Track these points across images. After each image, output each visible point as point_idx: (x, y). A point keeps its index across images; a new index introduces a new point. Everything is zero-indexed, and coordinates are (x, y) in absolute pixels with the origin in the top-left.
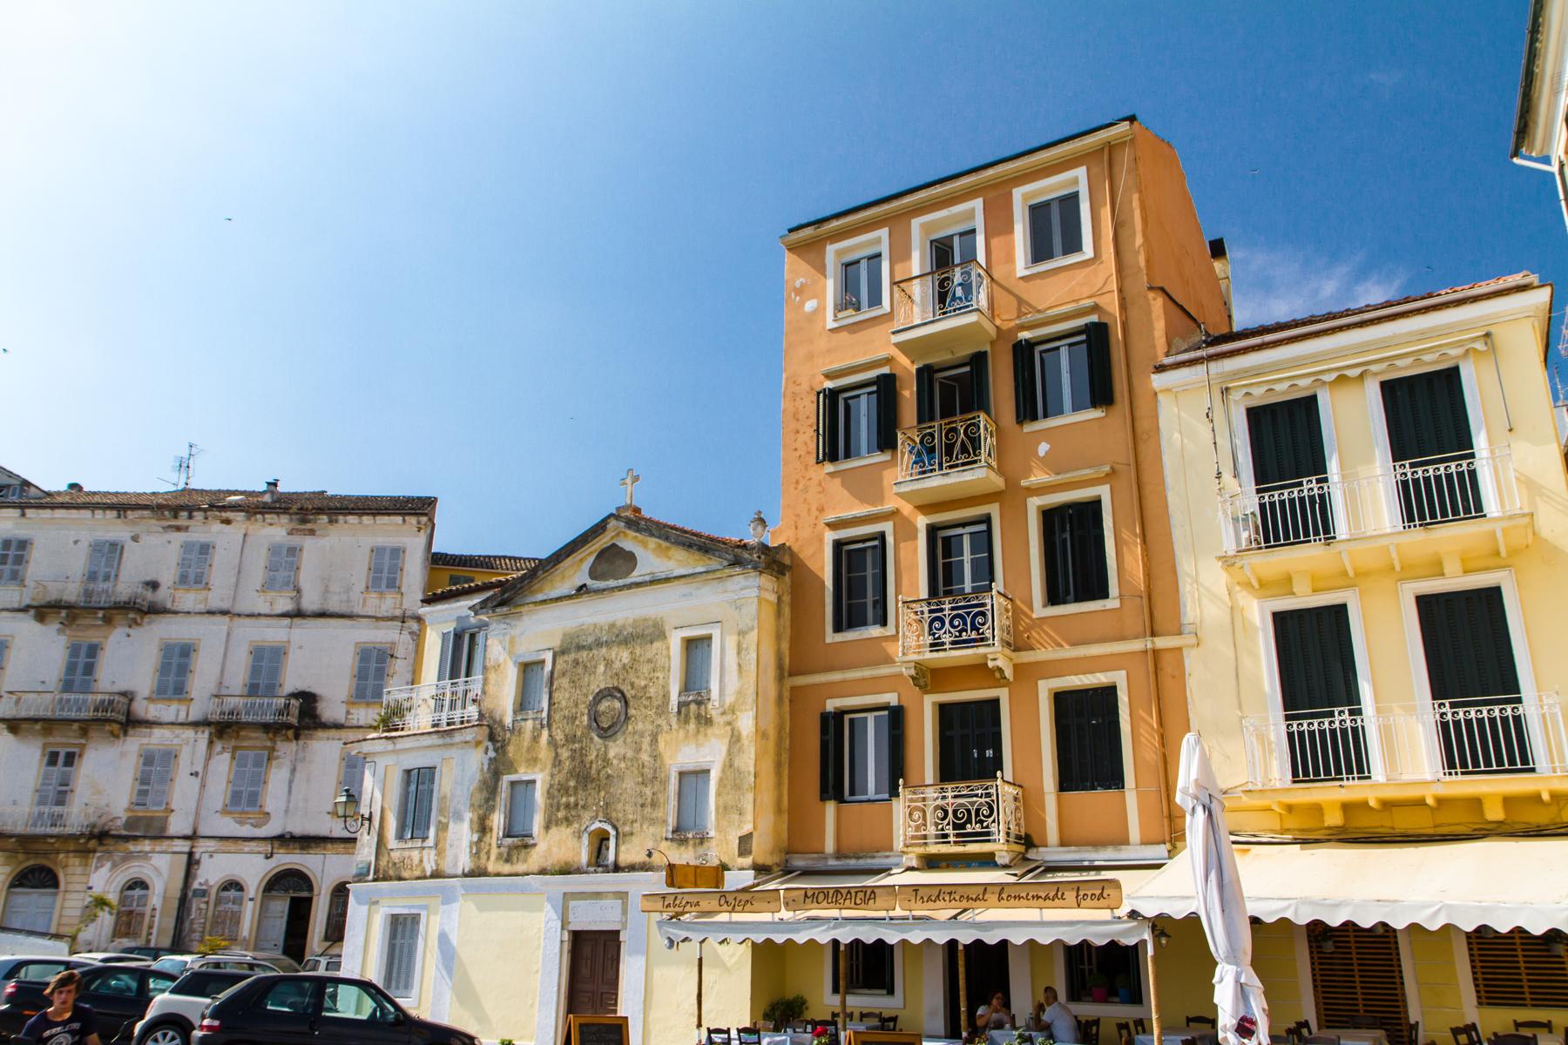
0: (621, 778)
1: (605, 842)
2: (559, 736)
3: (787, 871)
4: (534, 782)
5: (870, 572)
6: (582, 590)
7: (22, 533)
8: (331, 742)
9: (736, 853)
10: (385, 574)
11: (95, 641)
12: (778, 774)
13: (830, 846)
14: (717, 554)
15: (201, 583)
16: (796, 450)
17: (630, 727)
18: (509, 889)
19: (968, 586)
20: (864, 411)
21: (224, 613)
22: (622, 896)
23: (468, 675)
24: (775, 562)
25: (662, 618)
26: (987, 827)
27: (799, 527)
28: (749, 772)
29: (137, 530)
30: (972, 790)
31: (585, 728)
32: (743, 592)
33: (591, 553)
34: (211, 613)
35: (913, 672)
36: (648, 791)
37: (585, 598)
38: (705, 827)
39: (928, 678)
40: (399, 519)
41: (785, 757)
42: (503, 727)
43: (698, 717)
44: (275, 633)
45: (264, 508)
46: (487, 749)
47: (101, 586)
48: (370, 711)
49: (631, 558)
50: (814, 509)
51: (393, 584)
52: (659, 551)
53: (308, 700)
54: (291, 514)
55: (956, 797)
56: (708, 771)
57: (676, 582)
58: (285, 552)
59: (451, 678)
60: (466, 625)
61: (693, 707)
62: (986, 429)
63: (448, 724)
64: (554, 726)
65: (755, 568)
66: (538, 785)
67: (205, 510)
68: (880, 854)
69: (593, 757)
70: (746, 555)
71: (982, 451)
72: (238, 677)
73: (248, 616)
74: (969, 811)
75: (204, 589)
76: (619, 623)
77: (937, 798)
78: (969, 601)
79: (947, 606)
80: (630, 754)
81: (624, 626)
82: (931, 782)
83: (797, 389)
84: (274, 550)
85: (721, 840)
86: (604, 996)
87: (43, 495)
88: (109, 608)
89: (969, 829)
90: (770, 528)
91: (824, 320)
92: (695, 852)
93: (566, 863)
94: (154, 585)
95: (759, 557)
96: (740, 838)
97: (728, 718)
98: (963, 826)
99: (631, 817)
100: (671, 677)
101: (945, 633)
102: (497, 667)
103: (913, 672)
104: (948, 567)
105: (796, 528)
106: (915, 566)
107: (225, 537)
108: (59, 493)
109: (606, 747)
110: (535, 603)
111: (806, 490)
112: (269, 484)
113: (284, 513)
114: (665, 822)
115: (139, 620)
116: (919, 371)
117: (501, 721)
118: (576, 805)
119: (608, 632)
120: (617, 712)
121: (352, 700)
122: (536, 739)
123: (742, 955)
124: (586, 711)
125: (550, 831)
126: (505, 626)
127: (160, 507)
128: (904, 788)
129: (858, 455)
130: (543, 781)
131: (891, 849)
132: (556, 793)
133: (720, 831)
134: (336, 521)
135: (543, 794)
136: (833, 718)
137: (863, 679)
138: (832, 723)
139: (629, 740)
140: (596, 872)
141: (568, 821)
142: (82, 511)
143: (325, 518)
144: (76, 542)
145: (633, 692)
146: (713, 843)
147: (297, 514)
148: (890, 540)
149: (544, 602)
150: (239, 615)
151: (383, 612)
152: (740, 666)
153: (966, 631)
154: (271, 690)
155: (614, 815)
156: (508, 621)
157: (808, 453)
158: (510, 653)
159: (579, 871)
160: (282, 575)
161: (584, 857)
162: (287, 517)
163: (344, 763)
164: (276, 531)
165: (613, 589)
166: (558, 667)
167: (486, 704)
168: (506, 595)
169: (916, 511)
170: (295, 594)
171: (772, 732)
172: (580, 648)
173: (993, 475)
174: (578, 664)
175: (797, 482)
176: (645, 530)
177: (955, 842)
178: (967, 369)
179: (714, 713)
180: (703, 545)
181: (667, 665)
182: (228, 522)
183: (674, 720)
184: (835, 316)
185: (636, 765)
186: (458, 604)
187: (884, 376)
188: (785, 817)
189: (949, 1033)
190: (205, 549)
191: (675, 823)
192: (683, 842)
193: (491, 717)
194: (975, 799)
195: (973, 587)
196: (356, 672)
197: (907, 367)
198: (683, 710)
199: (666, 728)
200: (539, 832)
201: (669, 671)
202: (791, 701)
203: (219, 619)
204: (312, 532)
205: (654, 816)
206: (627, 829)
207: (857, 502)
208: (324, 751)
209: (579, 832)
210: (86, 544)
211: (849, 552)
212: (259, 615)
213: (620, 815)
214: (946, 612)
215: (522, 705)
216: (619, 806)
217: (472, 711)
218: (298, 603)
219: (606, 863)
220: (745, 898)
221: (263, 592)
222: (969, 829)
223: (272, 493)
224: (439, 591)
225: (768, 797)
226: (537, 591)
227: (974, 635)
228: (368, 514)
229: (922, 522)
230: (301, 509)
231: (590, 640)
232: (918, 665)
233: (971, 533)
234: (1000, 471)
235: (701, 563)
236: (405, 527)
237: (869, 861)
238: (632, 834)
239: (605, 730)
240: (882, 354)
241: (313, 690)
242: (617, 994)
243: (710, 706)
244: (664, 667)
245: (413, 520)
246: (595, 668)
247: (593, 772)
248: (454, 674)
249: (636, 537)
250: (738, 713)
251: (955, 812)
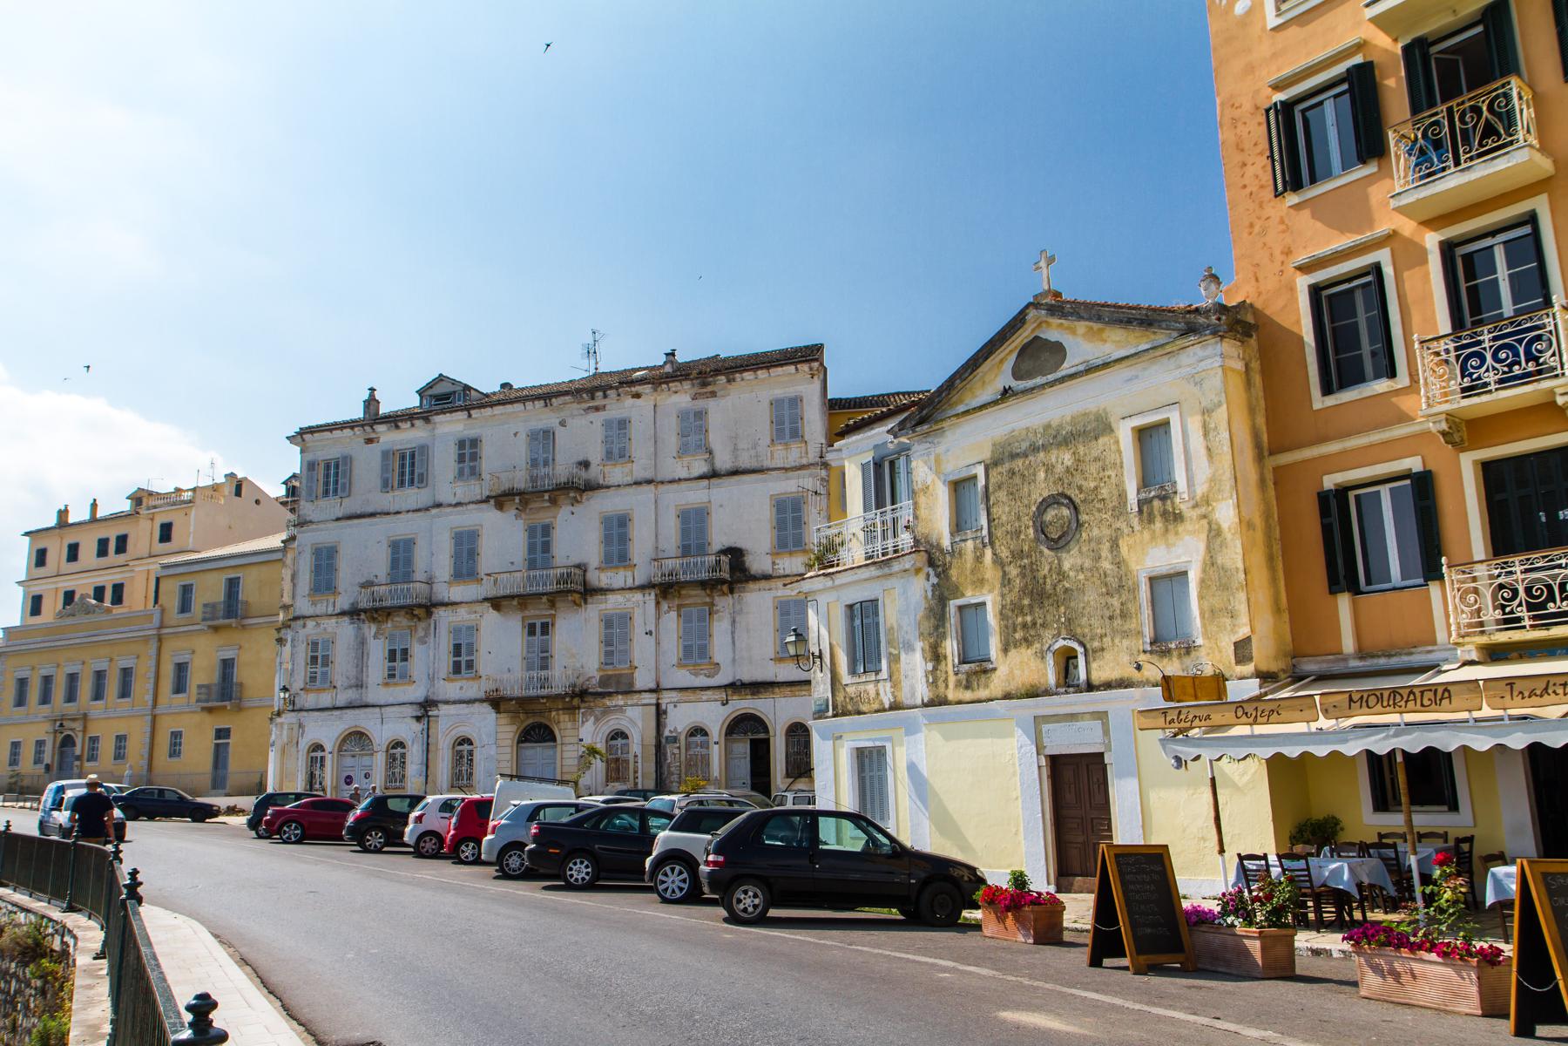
0: (1082, 591)
1: (1071, 661)
2: (1004, 553)
3: (1297, 678)
4: (984, 604)
5: (1362, 318)
6: (1006, 393)
7: (472, 433)
8: (763, 592)
9: (1233, 661)
10: (787, 426)
11: (547, 521)
12: (1272, 568)
13: (1348, 644)
14: (1164, 325)
15: (624, 456)
16: (1245, 186)
17: (1084, 535)
18: (972, 718)
19: (1508, 308)
20: (1332, 122)
21: (649, 482)
22: (1102, 716)
23: (893, 503)
24: (1238, 322)
25: (1104, 409)
26: (1512, 612)
27: (1261, 278)
28: (1237, 569)
29: (563, 414)
30: (1552, 560)
31: (1032, 541)
32: (1203, 363)
33: (1011, 351)
34: (637, 483)
35: (1444, 426)
36: (1115, 602)
37: (1012, 401)
38: (1189, 636)
39: (1463, 432)
40: (792, 368)
41: (1277, 548)
42: (941, 550)
43: (1165, 514)
44: (695, 495)
45: (667, 377)
46: (928, 575)
47: (543, 471)
48: (794, 559)
49: (1058, 350)
50: (1277, 253)
51: (796, 434)
52: (1091, 335)
53: (735, 555)
54: (692, 380)
55: (1527, 571)
56: (1185, 573)
57: (1117, 366)
58: (692, 416)
59: (877, 508)
60: (885, 452)
61: (1157, 504)
62: (1520, 98)
63: (883, 555)
64: (997, 543)
65: (1214, 333)
66: (989, 607)
67: (617, 388)
68: (1420, 649)
69: (1046, 571)
70: (1201, 320)
71: (1519, 128)
72: (671, 540)
73: (670, 482)
74: (1549, 587)
75: (628, 462)
76: (1054, 424)
77: (1499, 576)
78: (1519, 325)
79: (1486, 337)
80: (1088, 564)
81: (1061, 426)
82: (1483, 557)
83: (1237, 113)
84: (683, 416)
85: (1211, 648)
86: (1095, 821)
87: (482, 396)
88: (553, 490)
89: (1551, 607)
90: (1223, 287)
91: (1264, 18)
92: (1182, 664)
93: (1032, 686)
94: (585, 464)
95: (1219, 319)
96: (1235, 643)
97: (1203, 510)
98: (1543, 606)
99: (1099, 631)
100: (1125, 473)
101: (1487, 370)
102: (926, 489)
103: (1444, 426)
104: (1473, 292)
105: (1257, 280)
106: (1428, 297)
107: (636, 409)
108: (494, 394)
109: (1059, 560)
110: (957, 415)
111: (1264, 232)
112: (667, 354)
113: (686, 379)
114: (1140, 633)
115: (579, 498)
116: (1407, 50)
117: (938, 544)
118: (1034, 624)
119: (1043, 435)
120: (1066, 519)
121: (774, 551)
122: (979, 559)
123: (1256, 772)
124: (1031, 523)
125: (1010, 654)
126: (928, 445)
127: (578, 391)
128: (1449, 567)
129: (1328, 175)
130: (994, 603)
131: (1434, 643)
132: (1010, 614)
133: (1208, 638)
134: (734, 380)
135: (995, 616)
136: (1334, 496)
137: (1371, 446)
138: (1333, 503)
139: (1084, 549)
140: (1067, 693)
141: (1028, 642)
142: (515, 405)
143: (722, 379)
144: (515, 434)
145: (1082, 496)
146: (1203, 652)
147: (697, 378)
148: (1388, 271)
149: (967, 413)
150: (662, 483)
151: (791, 463)
152: (1209, 449)
153: (1519, 363)
154: (702, 549)
155: (1079, 631)
156: (930, 440)
157: (1262, 187)
158: (938, 473)
159: (1047, 693)
160: (693, 439)
161: (1051, 678)
162: (689, 382)
163: (778, 612)
164: (680, 398)
165: (1043, 386)
166: (992, 480)
167: (919, 529)
168: (924, 412)
169: (1422, 227)
170: (707, 456)
171: (1258, 521)
172: (1013, 456)
173: (1538, 157)
174: (1014, 473)
175: (1251, 225)
176: (1072, 314)
177: (1531, 626)
178: (1480, 29)
179: (1183, 507)
180: (1145, 319)
181: (1118, 461)
182: (637, 396)
183: (1135, 522)
184: (1278, 9)
185: (1096, 575)
186: (873, 432)
187: (1358, 67)
188: (1286, 616)
189: (1542, 854)
190: (623, 424)
191: (1152, 635)
192: (1166, 653)
193: (928, 542)
194: (1557, 571)
195: (1515, 310)
196: (774, 524)
197: (1388, 47)
198: (1145, 509)
199: (1126, 530)
200: (997, 655)
201: (1122, 467)
202: (1275, 484)
203: (646, 488)
204: (713, 394)
205: (1126, 628)
206: (1096, 644)
207: (1336, 232)
208: (759, 603)
209: (1042, 652)
210: (524, 436)
211: (1330, 297)
212: (680, 480)
213: (1086, 630)
214: (1486, 345)
215: (958, 526)
216: (1084, 621)
217: (905, 539)
218: (713, 464)
219: (1076, 682)
220: (1252, 710)
221: (680, 457)
222: (1551, 607)
223: (672, 362)
224: (851, 422)
225: (1263, 596)
226: (956, 403)
227: (1531, 367)
228: (762, 368)
229: (1432, 241)
230: (700, 373)
231: (1024, 445)
232: (1450, 416)
233: (1505, 243)
234: (1544, 149)
235: (1145, 339)
236: (798, 376)
237: (1405, 658)
238: (1103, 649)
239: (1056, 541)
240: (1350, 40)
241: (738, 545)
242: (1110, 819)
243: (1177, 500)
244: (1115, 464)
245: (805, 367)
246: (1035, 475)
247: (1048, 587)
248: (880, 504)
249: (1061, 324)
250: (1214, 504)
251: (1528, 590)
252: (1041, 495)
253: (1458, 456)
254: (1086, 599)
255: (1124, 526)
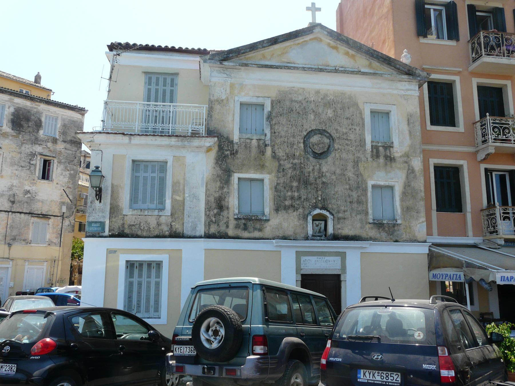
36: (354, 195)
99: (343, 208)
118: (300, 198)
124: (302, 141)
130: (271, 181)
132: (282, 189)
145: (338, 135)
200: (270, 212)
206: (341, 215)
213: (335, 207)
252: (310, 127)
253: (479, 165)
254: (336, 189)
255: (362, 156)
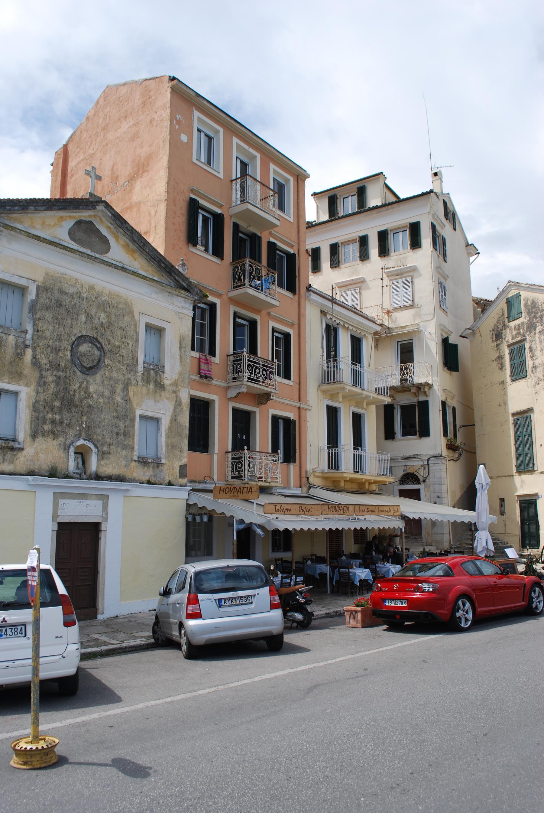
36: (121, 424)
69: (76, 386)
109: (88, 382)
124: (69, 348)
125: (37, 440)
132: (42, 409)
141: (54, 435)
199: (134, 382)
205: (126, 443)
206: (105, 449)
216: (99, 431)
238: (109, 453)
